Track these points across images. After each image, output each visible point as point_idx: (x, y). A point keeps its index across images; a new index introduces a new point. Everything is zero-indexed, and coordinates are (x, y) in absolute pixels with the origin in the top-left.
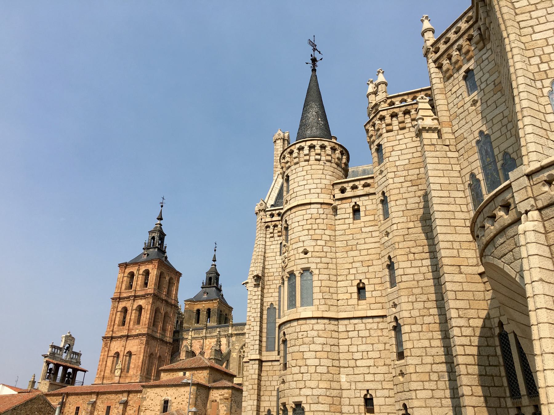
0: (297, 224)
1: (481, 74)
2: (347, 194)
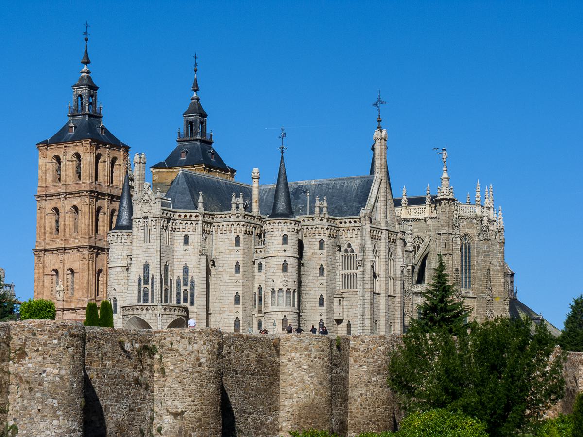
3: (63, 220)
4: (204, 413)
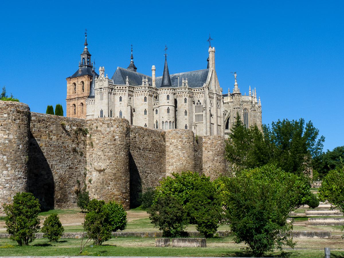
4: (118, 170)
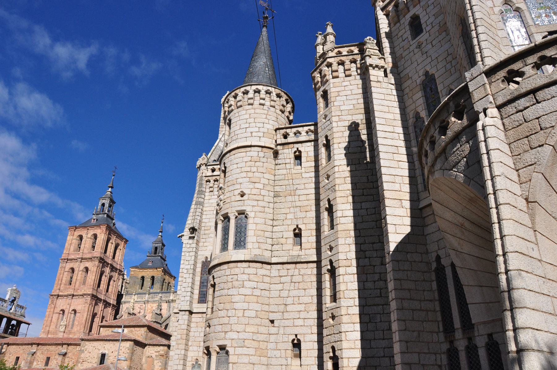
0: (235, 166)
1: (427, 17)
2: (290, 140)
3: (76, 276)
